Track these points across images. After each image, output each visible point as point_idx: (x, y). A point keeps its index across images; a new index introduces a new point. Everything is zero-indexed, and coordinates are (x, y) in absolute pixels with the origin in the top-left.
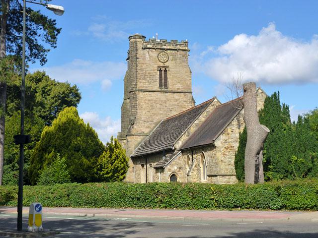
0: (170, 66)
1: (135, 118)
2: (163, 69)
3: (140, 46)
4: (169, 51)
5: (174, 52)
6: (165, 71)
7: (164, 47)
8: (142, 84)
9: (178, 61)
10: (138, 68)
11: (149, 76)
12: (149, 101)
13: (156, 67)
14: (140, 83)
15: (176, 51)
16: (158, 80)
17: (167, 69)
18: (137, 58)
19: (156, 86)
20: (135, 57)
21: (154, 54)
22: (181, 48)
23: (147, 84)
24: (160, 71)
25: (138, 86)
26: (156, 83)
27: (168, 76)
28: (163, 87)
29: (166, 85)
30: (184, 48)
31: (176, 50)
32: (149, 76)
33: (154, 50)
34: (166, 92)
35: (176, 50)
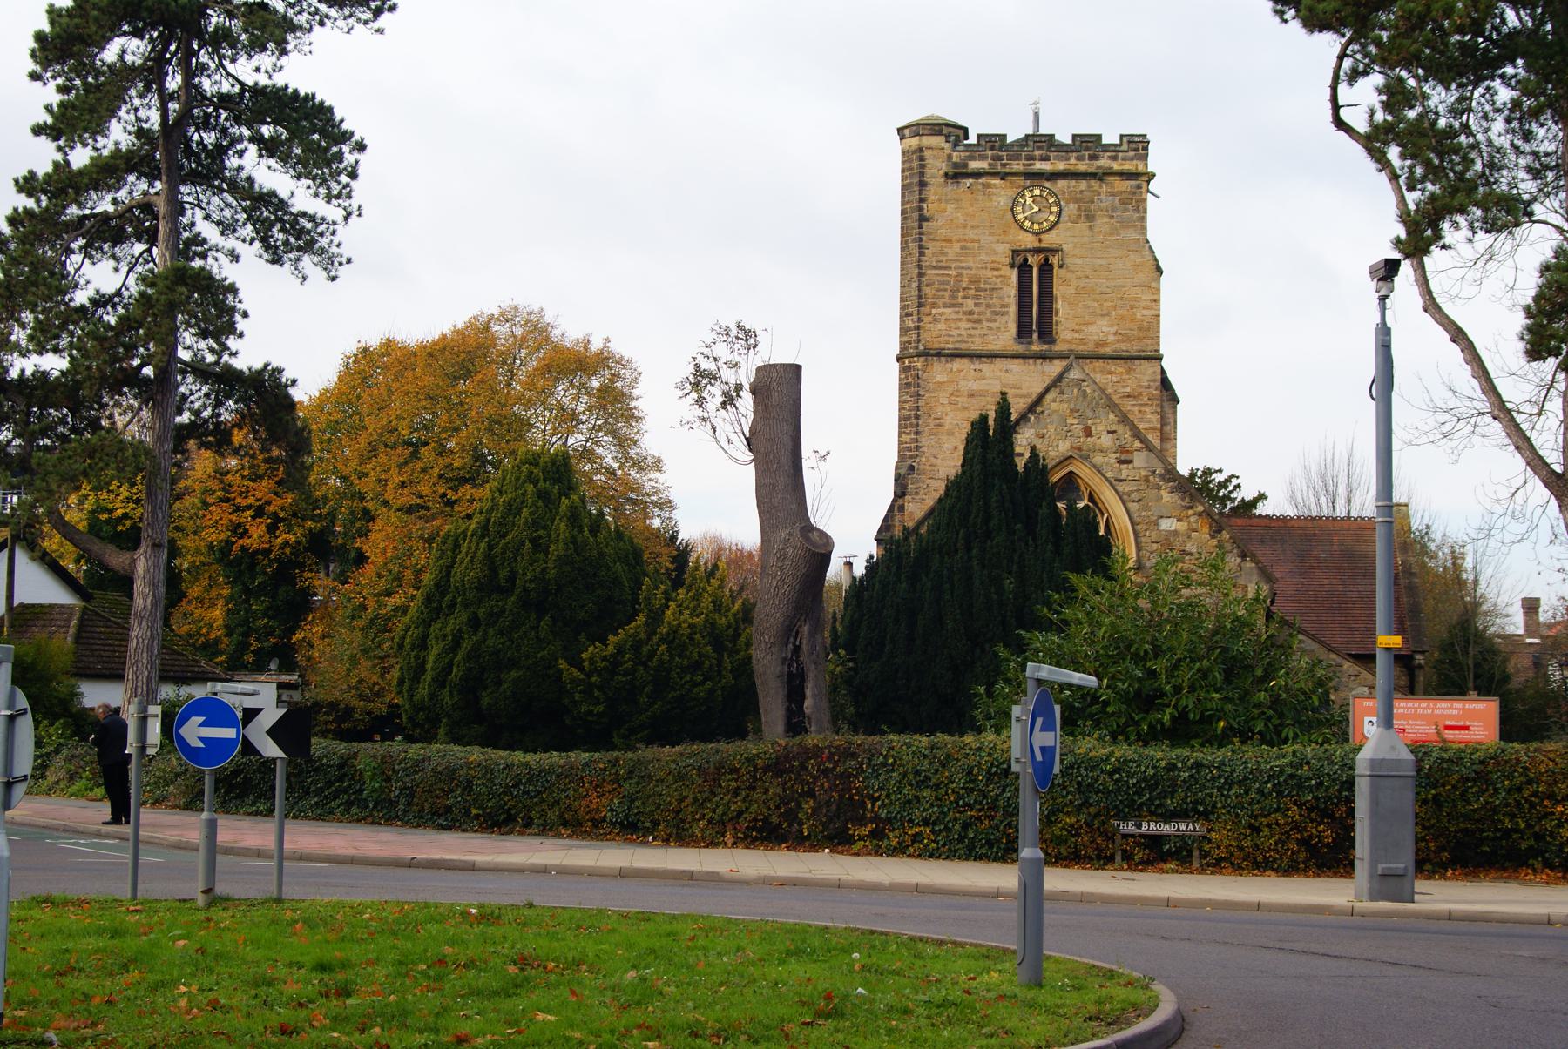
0: (1065, 247)
1: (912, 468)
2: (1034, 260)
3: (937, 167)
4: (1061, 183)
5: (1083, 184)
6: (1046, 268)
7: (1039, 166)
8: (941, 326)
9: (1102, 222)
10: (928, 259)
11: (973, 292)
12: (971, 396)
13: (1002, 252)
14: (936, 320)
15: (1093, 183)
16: (1013, 310)
17: (1054, 260)
18: (923, 218)
19: (1004, 334)
20: (916, 215)
21: (1002, 194)
22: (1116, 166)
23: (964, 325)
24: (1024, 269)
25: (924, 335)
26: (1001, 320)
27: (1058, 290)
28: (1035, 336)
29: (1046, 331)
30: (1129, 166)
31: (1093, 176)
32: (973, 292)
33: (997, 181)
34: (1044, 357)
35: (1093, 176)
